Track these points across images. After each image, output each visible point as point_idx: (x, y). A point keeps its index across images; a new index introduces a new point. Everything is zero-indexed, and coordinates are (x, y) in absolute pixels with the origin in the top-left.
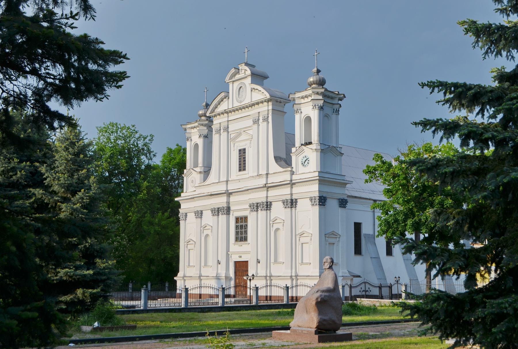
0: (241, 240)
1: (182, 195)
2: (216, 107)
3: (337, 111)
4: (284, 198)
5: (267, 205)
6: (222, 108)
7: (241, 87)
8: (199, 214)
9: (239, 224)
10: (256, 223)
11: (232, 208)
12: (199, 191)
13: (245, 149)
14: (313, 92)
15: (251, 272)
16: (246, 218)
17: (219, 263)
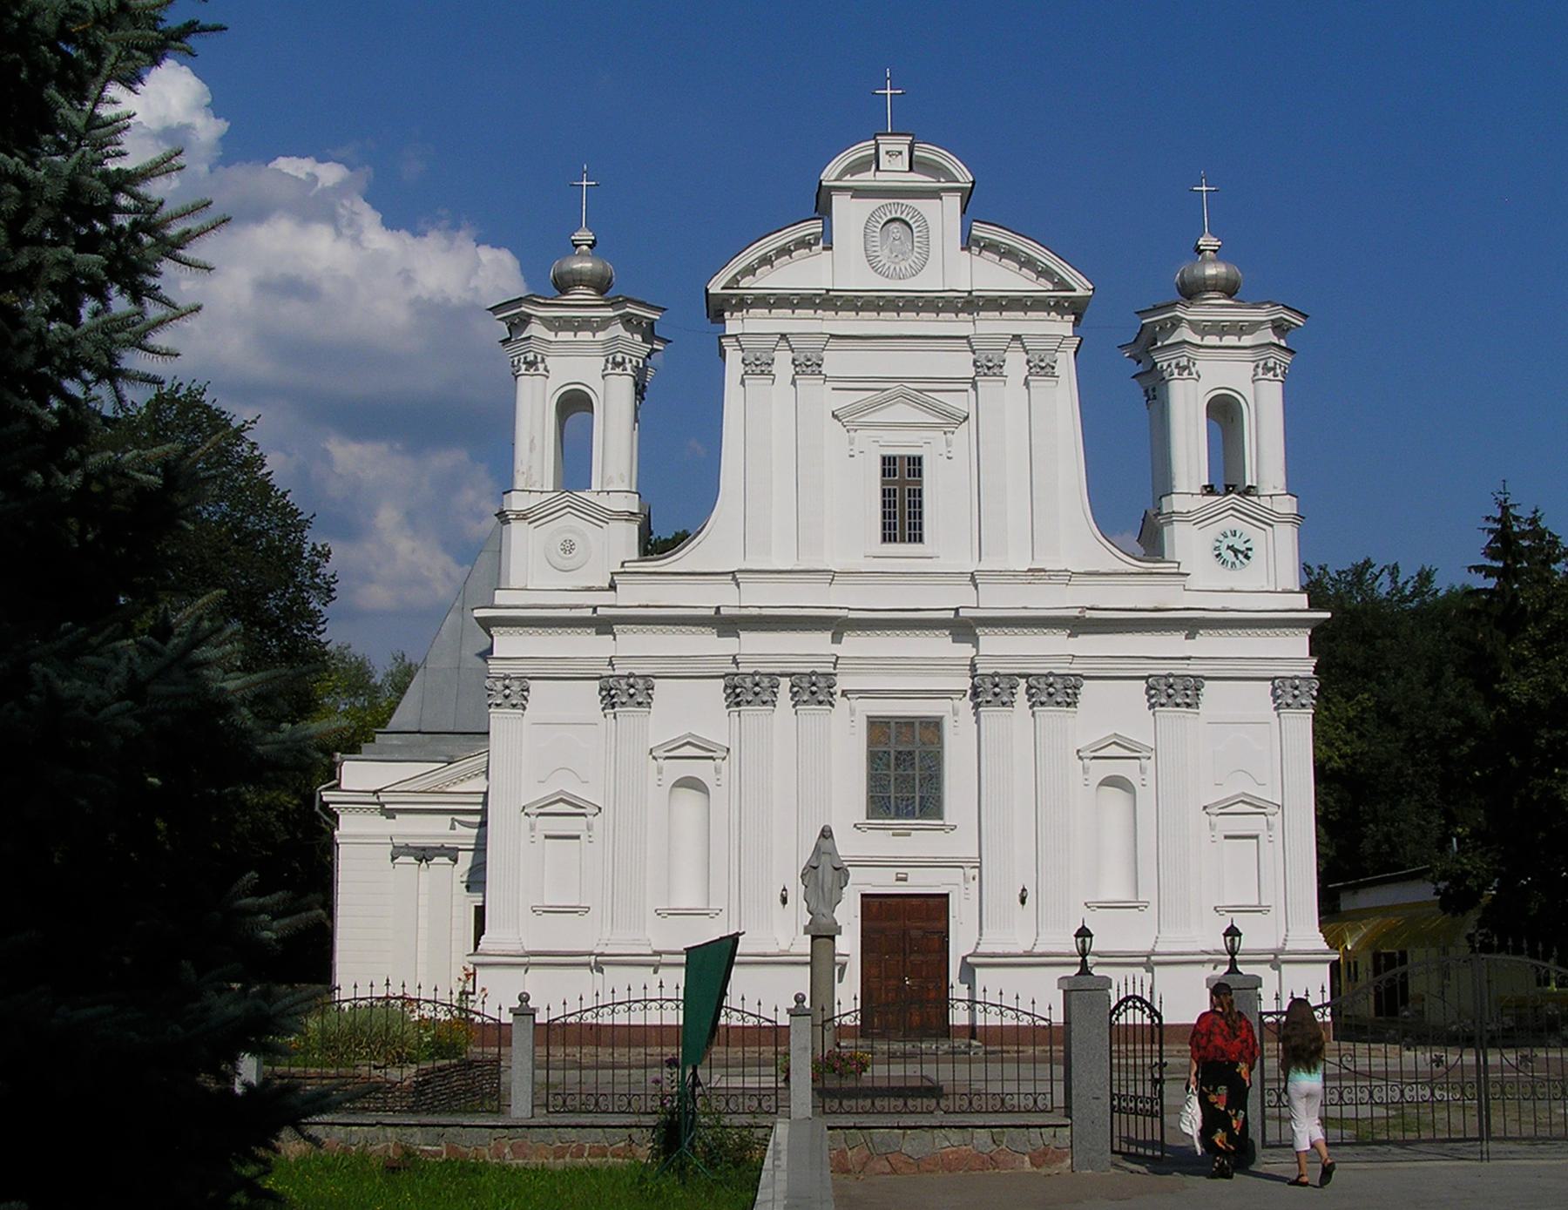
1: (500, 597)
2: (750, 270)
4: (1161, 669)
11: (842, 683)
12: (632, 596)
16: (934, 726)
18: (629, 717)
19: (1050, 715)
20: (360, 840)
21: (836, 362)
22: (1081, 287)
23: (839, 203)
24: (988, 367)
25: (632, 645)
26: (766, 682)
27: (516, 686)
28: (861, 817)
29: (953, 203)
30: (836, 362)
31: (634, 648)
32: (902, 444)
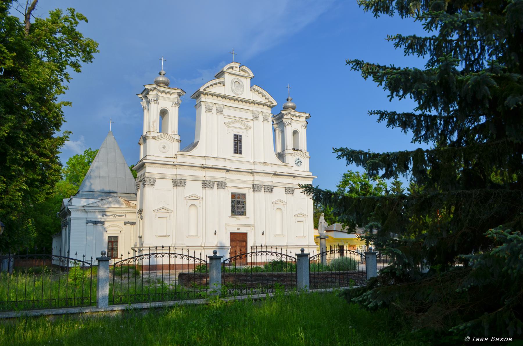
0: (238, 214)
2: (208, 87)
6: (212, 90)
9: (236, 200)
10: (252, 201)
16: (244, 195)
18: (180, 189)
19: (268, 194)
20: (78, 219)
22: (275, 103)
23: (226, 75)
24: (256, 118)
26: (211, 183)
27: (152, 180)
28: (230, 215)
29: (249, 80)
30: (226, 111)
31: (181, 173)
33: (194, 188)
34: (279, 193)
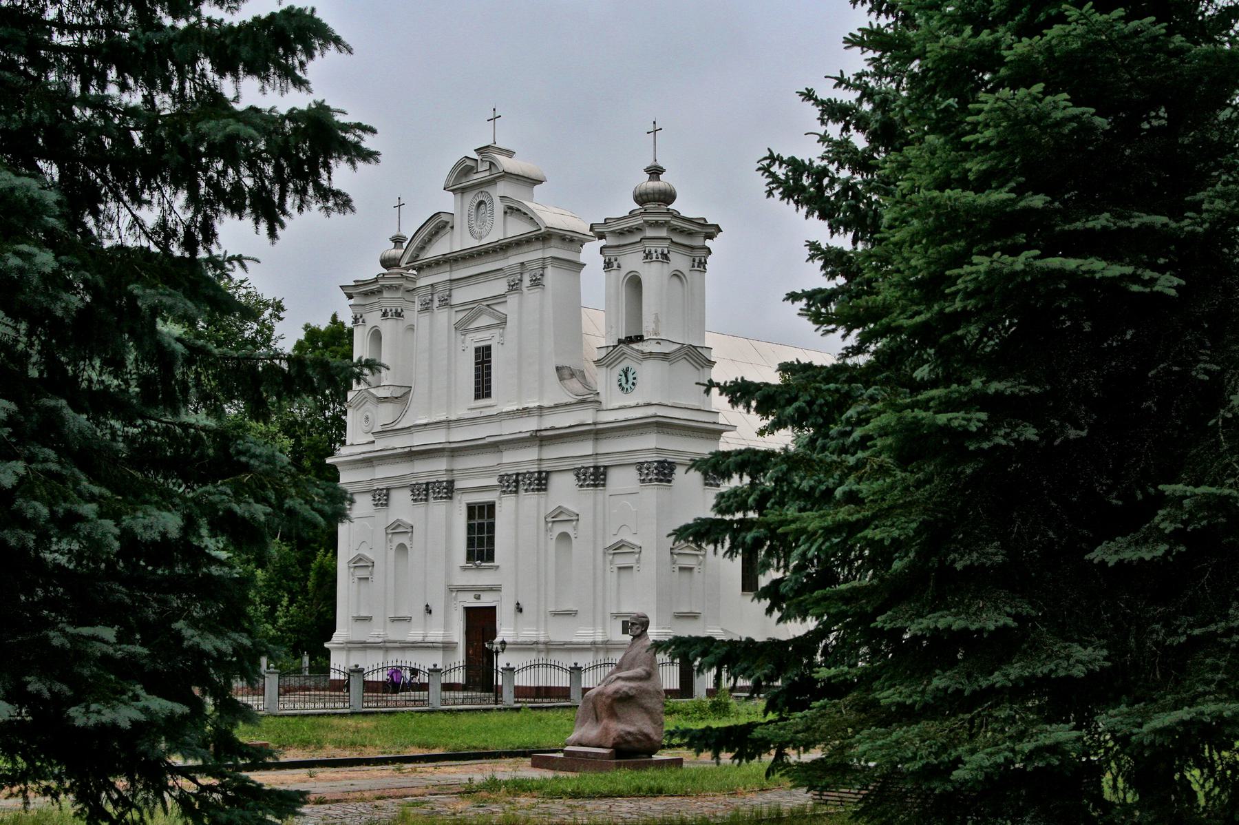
2: (422, 248)
3: (702, 264)
5: (539, 479)
7: (481, 203)
8: (382, 497)
9: (476, 521)
10: (514, 519)
11: (458, 485)
13: (489, 348)
14: (646, 222)
15: (505, 632)
16: (491, 506)
17: (429, 611)
21: (461, 295)
24: (514, 287)
25: (383, 472)
32: (481, 339)
33: (402, 506)
34: (564, 489)
